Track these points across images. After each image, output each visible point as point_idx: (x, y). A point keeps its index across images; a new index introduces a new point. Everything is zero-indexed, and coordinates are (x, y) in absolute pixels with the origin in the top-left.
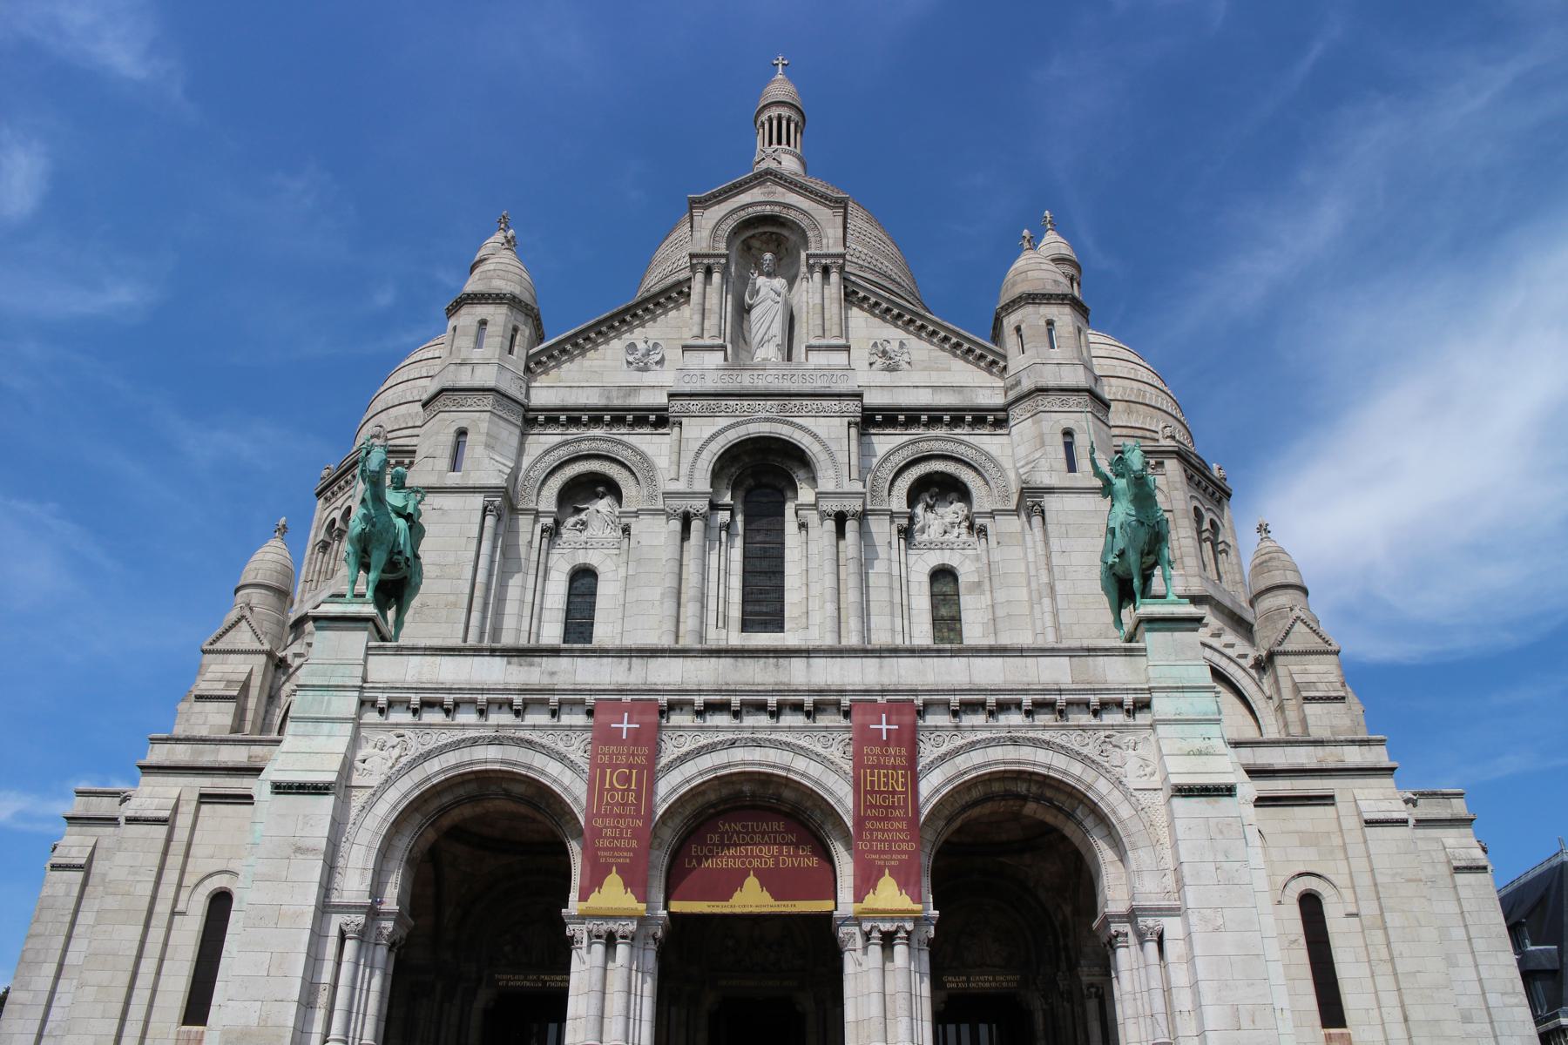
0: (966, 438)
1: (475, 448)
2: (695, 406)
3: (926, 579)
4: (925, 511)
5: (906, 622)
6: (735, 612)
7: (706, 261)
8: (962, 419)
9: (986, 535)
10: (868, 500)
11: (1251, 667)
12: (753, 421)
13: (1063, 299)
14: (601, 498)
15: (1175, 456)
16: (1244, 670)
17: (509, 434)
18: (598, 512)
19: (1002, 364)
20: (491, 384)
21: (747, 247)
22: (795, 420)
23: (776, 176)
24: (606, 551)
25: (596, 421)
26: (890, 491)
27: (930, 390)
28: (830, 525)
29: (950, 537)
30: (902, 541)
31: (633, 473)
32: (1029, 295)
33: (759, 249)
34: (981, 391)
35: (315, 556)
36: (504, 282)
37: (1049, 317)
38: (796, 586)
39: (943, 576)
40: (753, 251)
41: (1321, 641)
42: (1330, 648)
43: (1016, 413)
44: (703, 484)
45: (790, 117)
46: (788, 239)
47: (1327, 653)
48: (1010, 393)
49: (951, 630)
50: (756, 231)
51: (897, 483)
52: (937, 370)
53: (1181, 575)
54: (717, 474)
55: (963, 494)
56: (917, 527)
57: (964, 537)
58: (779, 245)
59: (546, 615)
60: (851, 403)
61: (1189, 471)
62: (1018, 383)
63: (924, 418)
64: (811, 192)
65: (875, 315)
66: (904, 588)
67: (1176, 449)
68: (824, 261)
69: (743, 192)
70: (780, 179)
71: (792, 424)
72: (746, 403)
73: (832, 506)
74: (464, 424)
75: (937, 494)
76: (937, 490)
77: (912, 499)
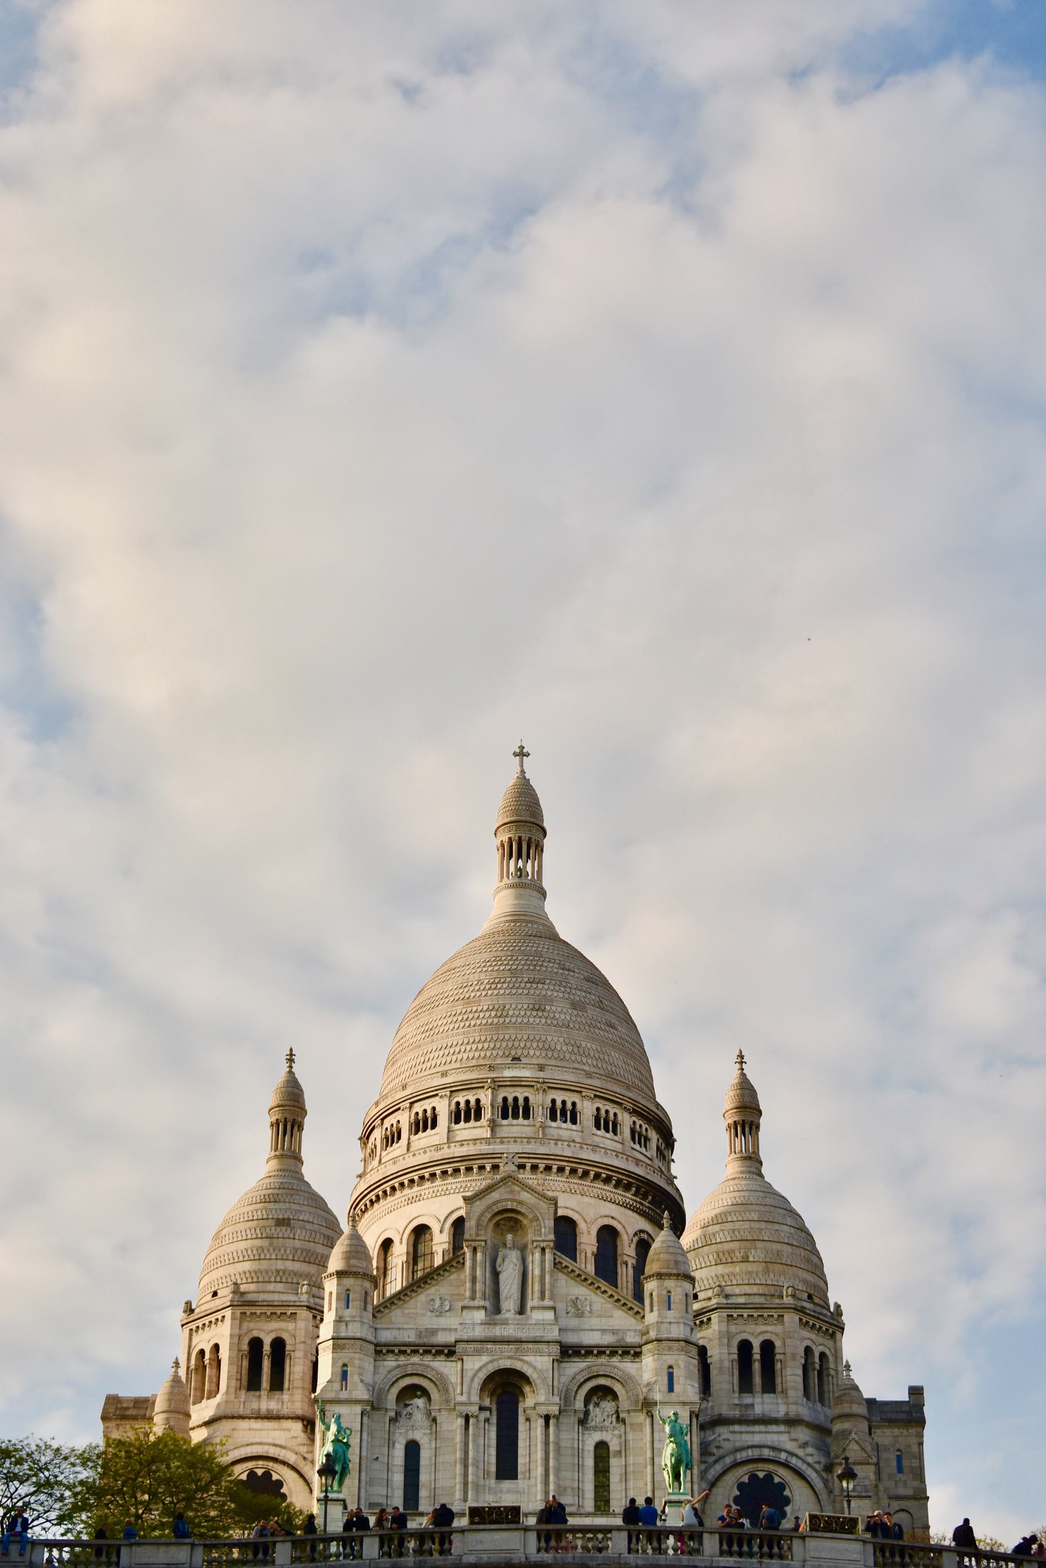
0: (618, 1364)
1: (353, 1378)
2: (471, 1347)
3: (592, 1448)
4: (594, 1406)
5: (580, 1474)
6: (493, 1469)
7: (473, 1244)
8: (617, 1352)
9: (625, 1424)
10: (562, 1405)
11: (823, 1470)
12: (500, 1359)
13: (678, 1277)
14: (419, 1398)
15: (792, 1310)
16: (817, 1472)
17: (368, 1364)
18: (418, 1407)
19: (642, 1315)
20: (358, 1335)
21: (497, 1225)
22: (525, 1358)
23: (514, 1179)
24: (423, 1431)
25: (415, 1352)
26: (575, 1397)
27: (599, 1333)
28: (541, 1422)
29: (606, 1423)
30: (580, 1427)
31: (436, 1385)
32: (658, 1274)
33: (504, 1225)
34: (629, 1333)
35: (190, 1376)
36: (357, 1261)
37: (669, 1288)
38: (524, 1454)
39: (602, 1447)
40: (501, 1226)
41: (866, 1455)
42: (870, 1461)
43: (645, 1348)
44: (475, 1398)
45: (530, 838)
46: (521, 1221)
47: (868, 1464)
48: (644, 1337)
49: (604, 1477)
50: (503, 1216)
51: (578, 1392)
52: (606, 1317)
53: (785, 1403)
54: (482, 1389)
55: (615, 1397)
56: (590, 1417)
57: (614, 1423)
58: (516, 1223)
59: (395, 1469)
60: (554, 1347)
61: (804, 1320)
62: (648, 1333)
63: (595, 1352)
64: (535, 1192)
65: (572, 1278)
66: (580, 1455)
67: (793, 1306)
68: (542, 1246)
69: (494, 1190)
70: (517, 1181)
71: (522, 1360)
72: (498, 1347)
73: (543, 1410)
74: (346, 1361)
75: (601, 1396)
76: (601, 1394)
77: (587, 1401)
